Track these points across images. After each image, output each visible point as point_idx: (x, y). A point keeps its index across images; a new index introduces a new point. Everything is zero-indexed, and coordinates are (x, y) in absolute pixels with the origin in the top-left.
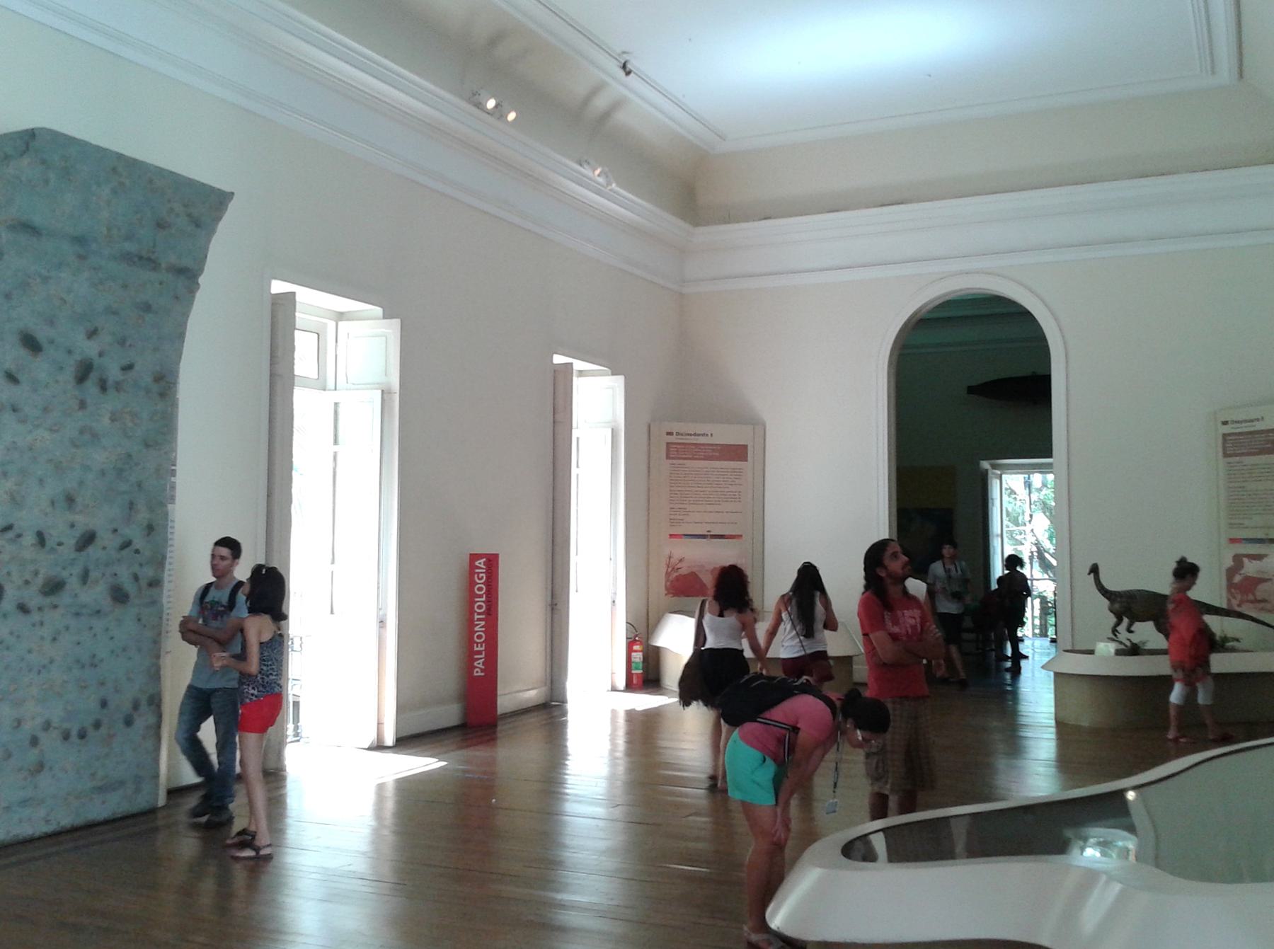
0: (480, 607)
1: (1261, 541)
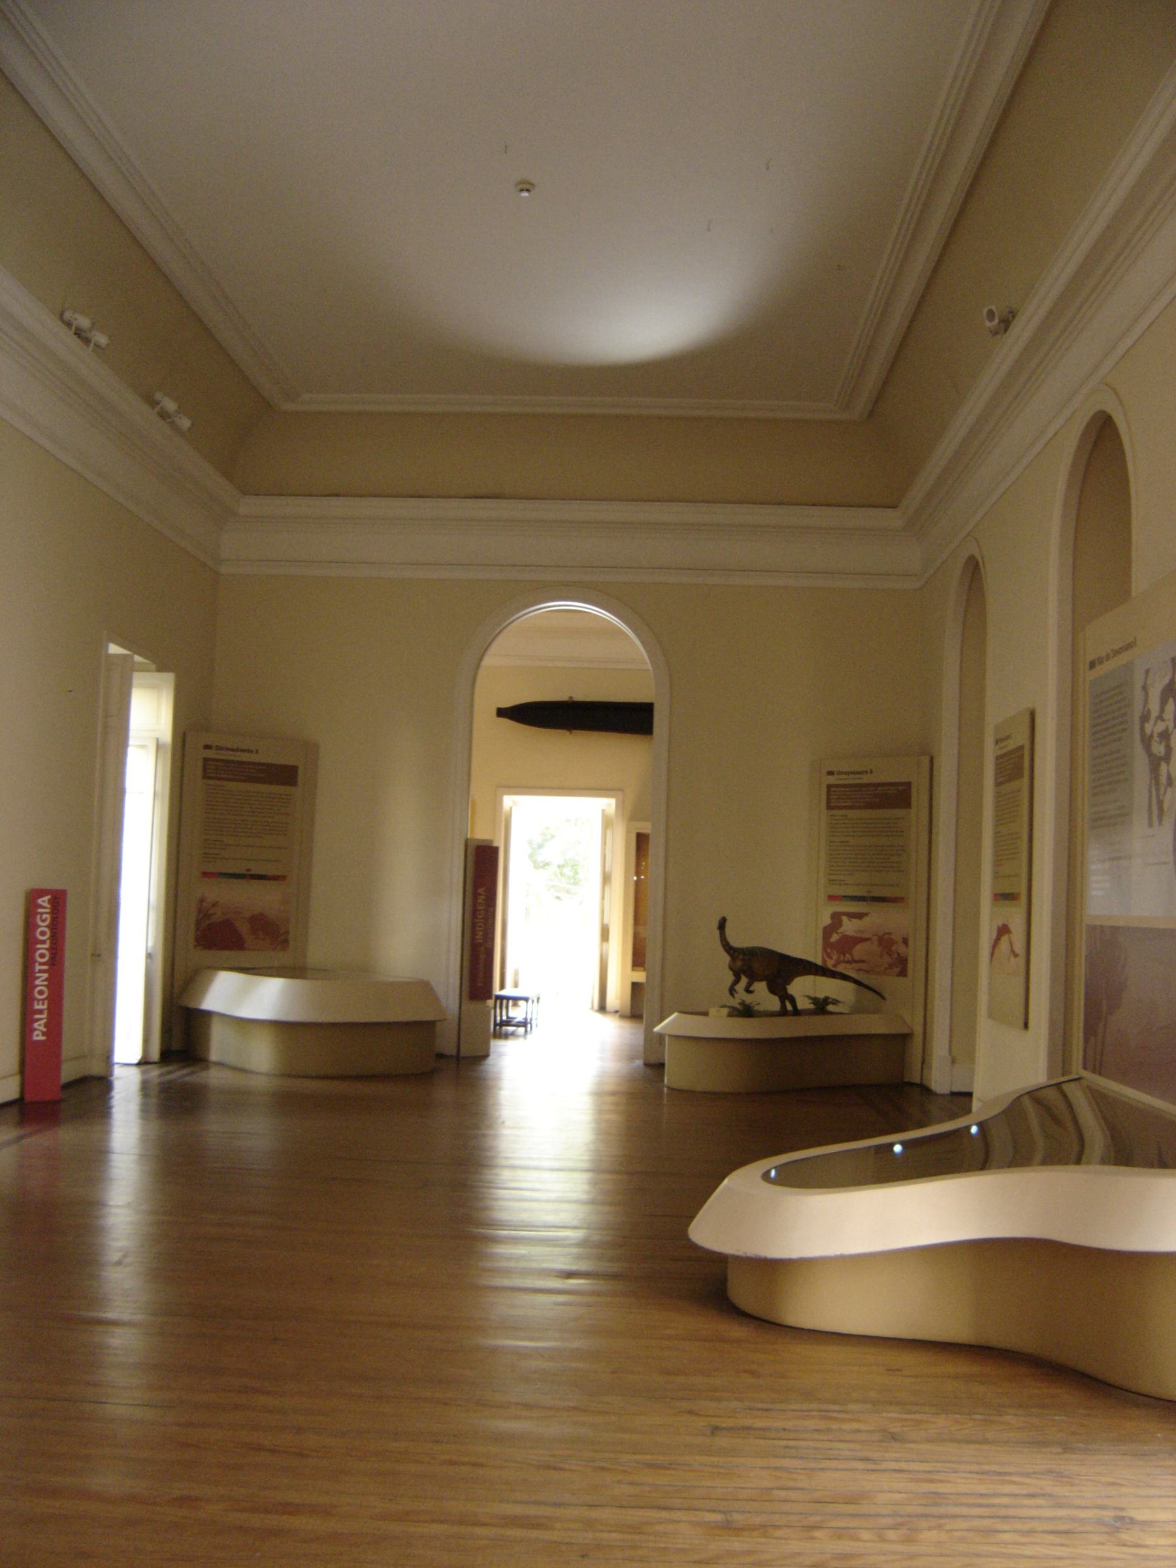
0: (42, 956)
1: (862, 899)
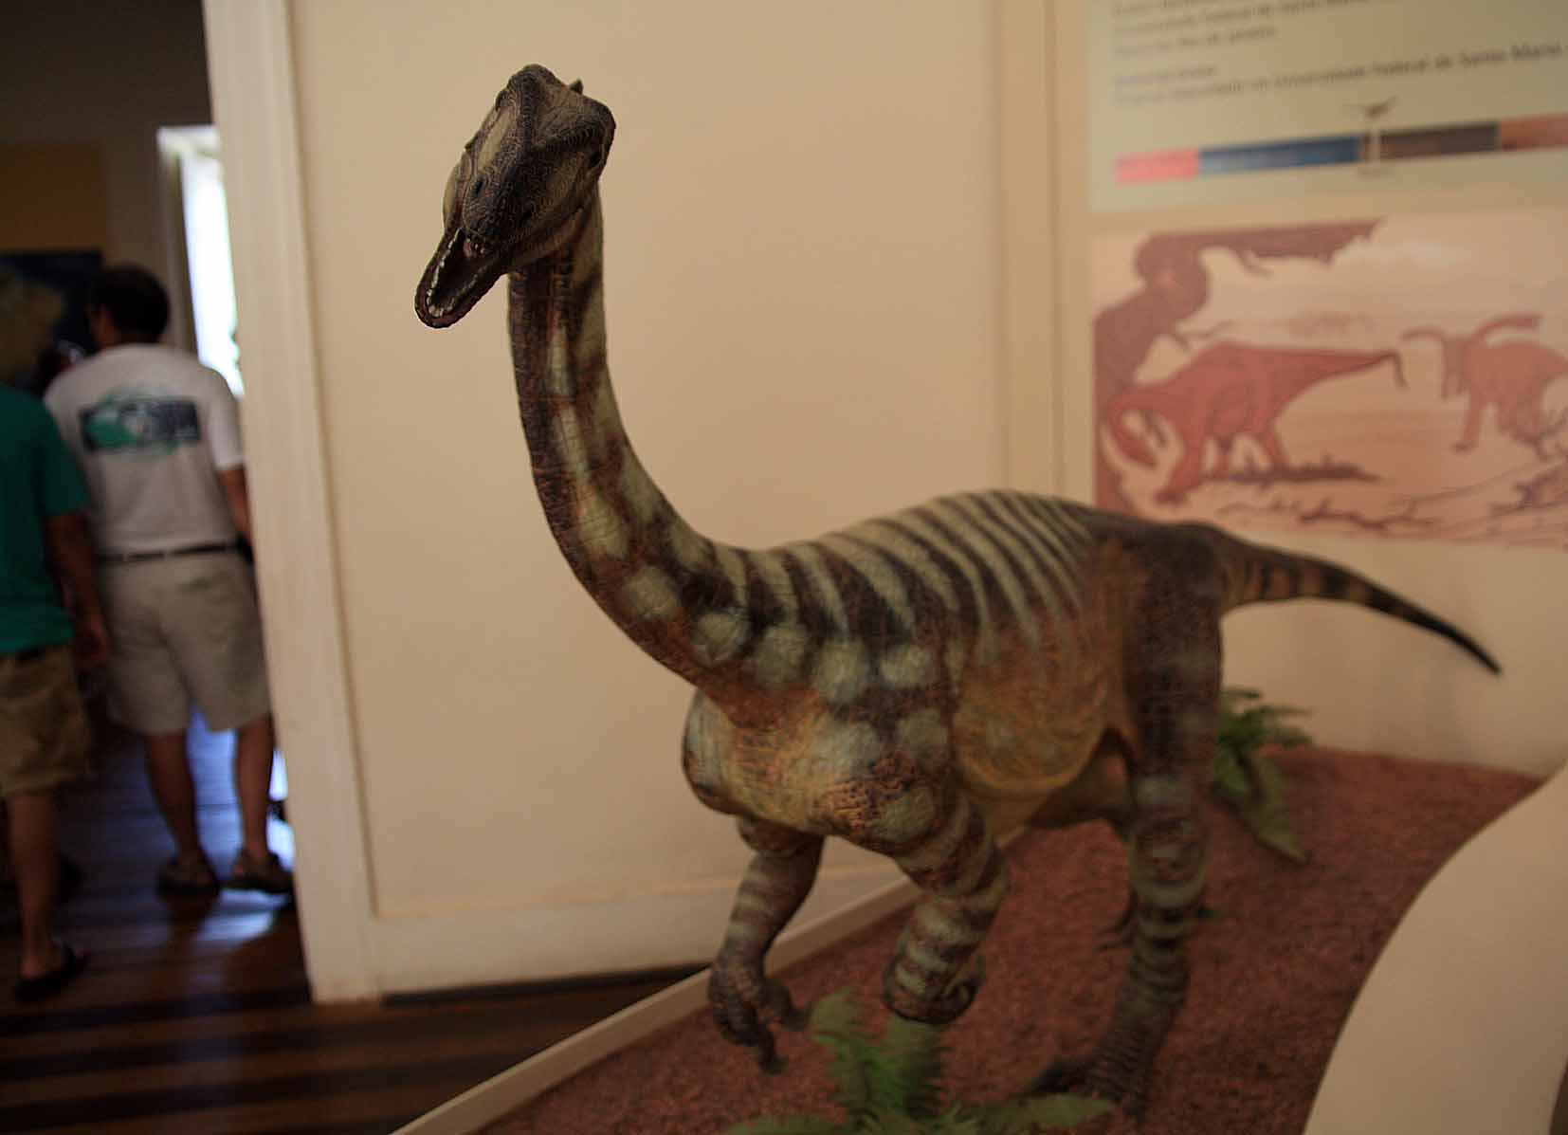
1: (1342, 150)
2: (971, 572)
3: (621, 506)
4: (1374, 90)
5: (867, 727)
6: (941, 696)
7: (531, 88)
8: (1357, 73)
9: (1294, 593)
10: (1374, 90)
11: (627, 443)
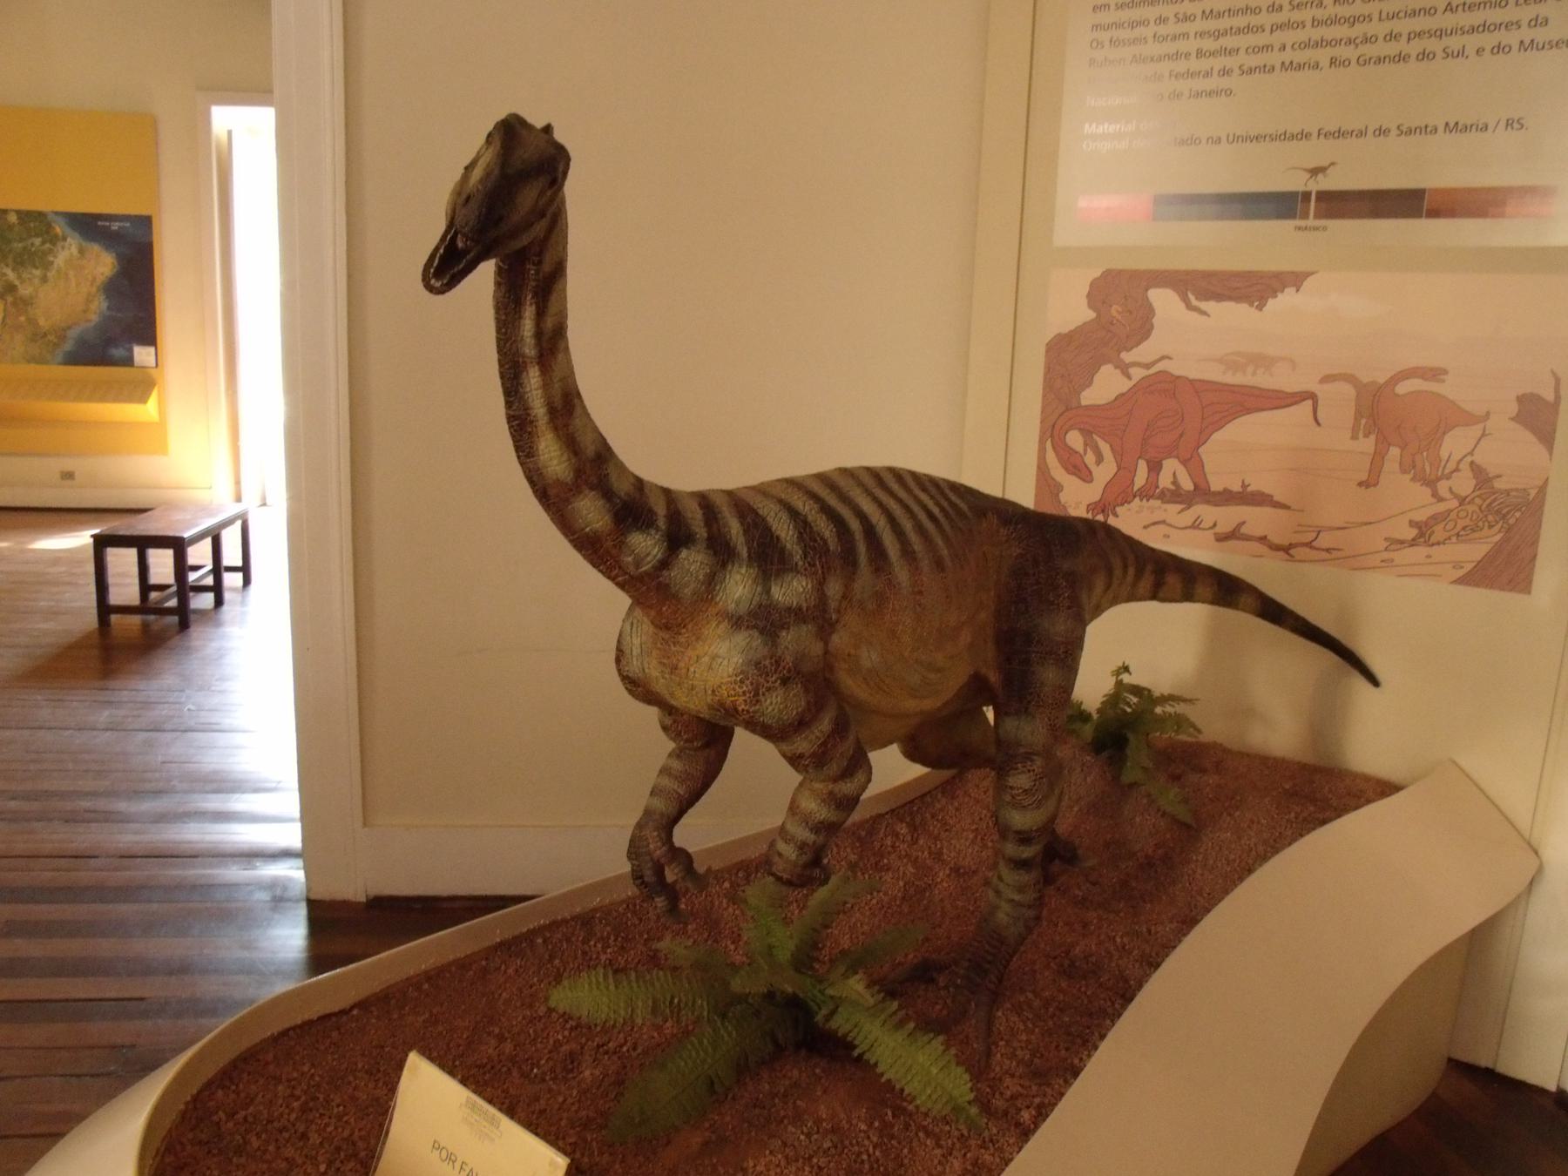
1: (1284, 205)
2: (855, 525)
3: (571, 444)
4: (1316, 151)
5: (756, 633)
6: (820, 617)
7: (510, 131)
8: (1304, 136)
9: (1188, 597)
10: (1316, 151)
11: (579, 394)
